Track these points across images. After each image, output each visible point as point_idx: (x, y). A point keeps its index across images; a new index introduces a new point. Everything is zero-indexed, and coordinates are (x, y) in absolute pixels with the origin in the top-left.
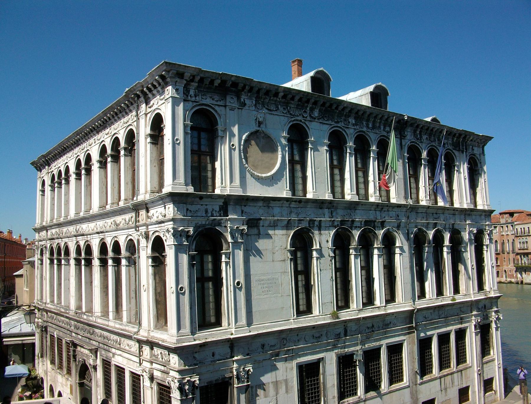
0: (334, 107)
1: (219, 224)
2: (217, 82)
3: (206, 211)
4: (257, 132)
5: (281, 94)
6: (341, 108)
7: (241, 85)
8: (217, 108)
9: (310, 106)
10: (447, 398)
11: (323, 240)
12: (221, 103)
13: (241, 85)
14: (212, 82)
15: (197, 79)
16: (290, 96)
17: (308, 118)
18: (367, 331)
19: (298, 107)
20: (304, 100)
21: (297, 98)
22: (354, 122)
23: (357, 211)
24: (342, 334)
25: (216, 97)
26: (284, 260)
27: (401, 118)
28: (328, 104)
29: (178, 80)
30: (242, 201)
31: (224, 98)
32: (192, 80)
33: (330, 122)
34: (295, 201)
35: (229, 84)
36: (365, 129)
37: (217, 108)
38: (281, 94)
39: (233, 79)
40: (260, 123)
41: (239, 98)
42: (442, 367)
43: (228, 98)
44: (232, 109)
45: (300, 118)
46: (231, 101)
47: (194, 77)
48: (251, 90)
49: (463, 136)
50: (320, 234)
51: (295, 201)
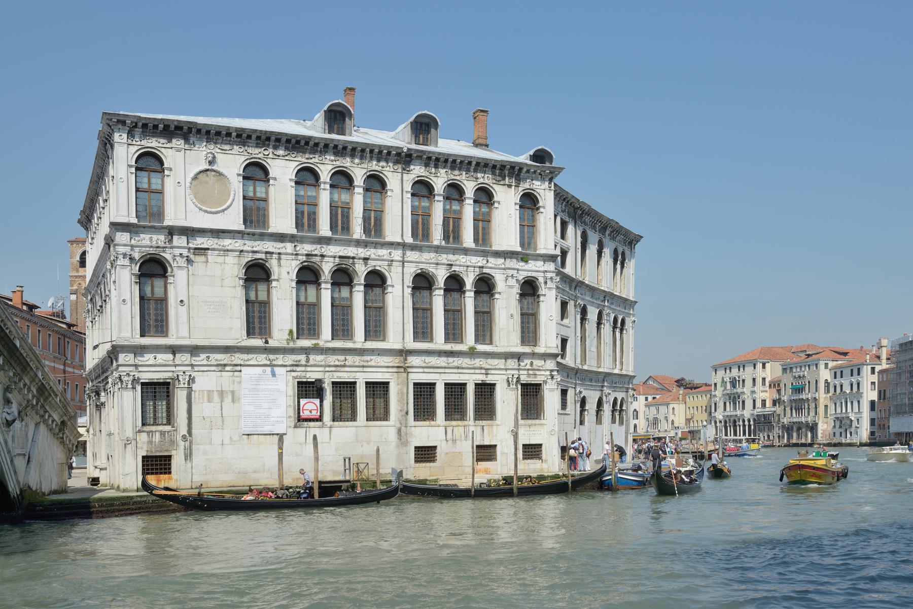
0: (302, 143)
1: (164, 251)
2: (161, 126)
3: (151, 239)
4: (207, 170)
5: (234, 134)
6: (312, 143)
7: (185, 128)
8: (163, 150)
9: (272, 143)
10: (454, 450)
11: (285, 273)
12: (169, 145)
13: (185, 128)
14: (156, 127)
15: (140, 124)
16: (245, 135)
17: (271, 156)
18: (337, 363)
19: (257, 146)
20: (263, 137)
21: (254, 137)
22: (333, 158)
23: (330, 247)
24: (303, 363)
25: (162, 141)
26: (235, 287)
27: (400, 151)
28: (293, 141)
29: (120, 126)
30: (189, 232)
31: (170, 141)
32: (136, 126)
33: (299, 159)
34: (248, 234)
35: (172, 127)
36: (348, 164)
37: (163, 150)
38: (234, 134)
39: (176, 123)
40: (210, 163)
41: (187, 140)
42: (449, 416)
43: (174, 141)
44: (179, 150)
45: (261, 156)
46: (178, 143)
47: (136, 123)
48: (199, 131)
49: (517, 168)
50: (280, 265)
51: (248, 234)
